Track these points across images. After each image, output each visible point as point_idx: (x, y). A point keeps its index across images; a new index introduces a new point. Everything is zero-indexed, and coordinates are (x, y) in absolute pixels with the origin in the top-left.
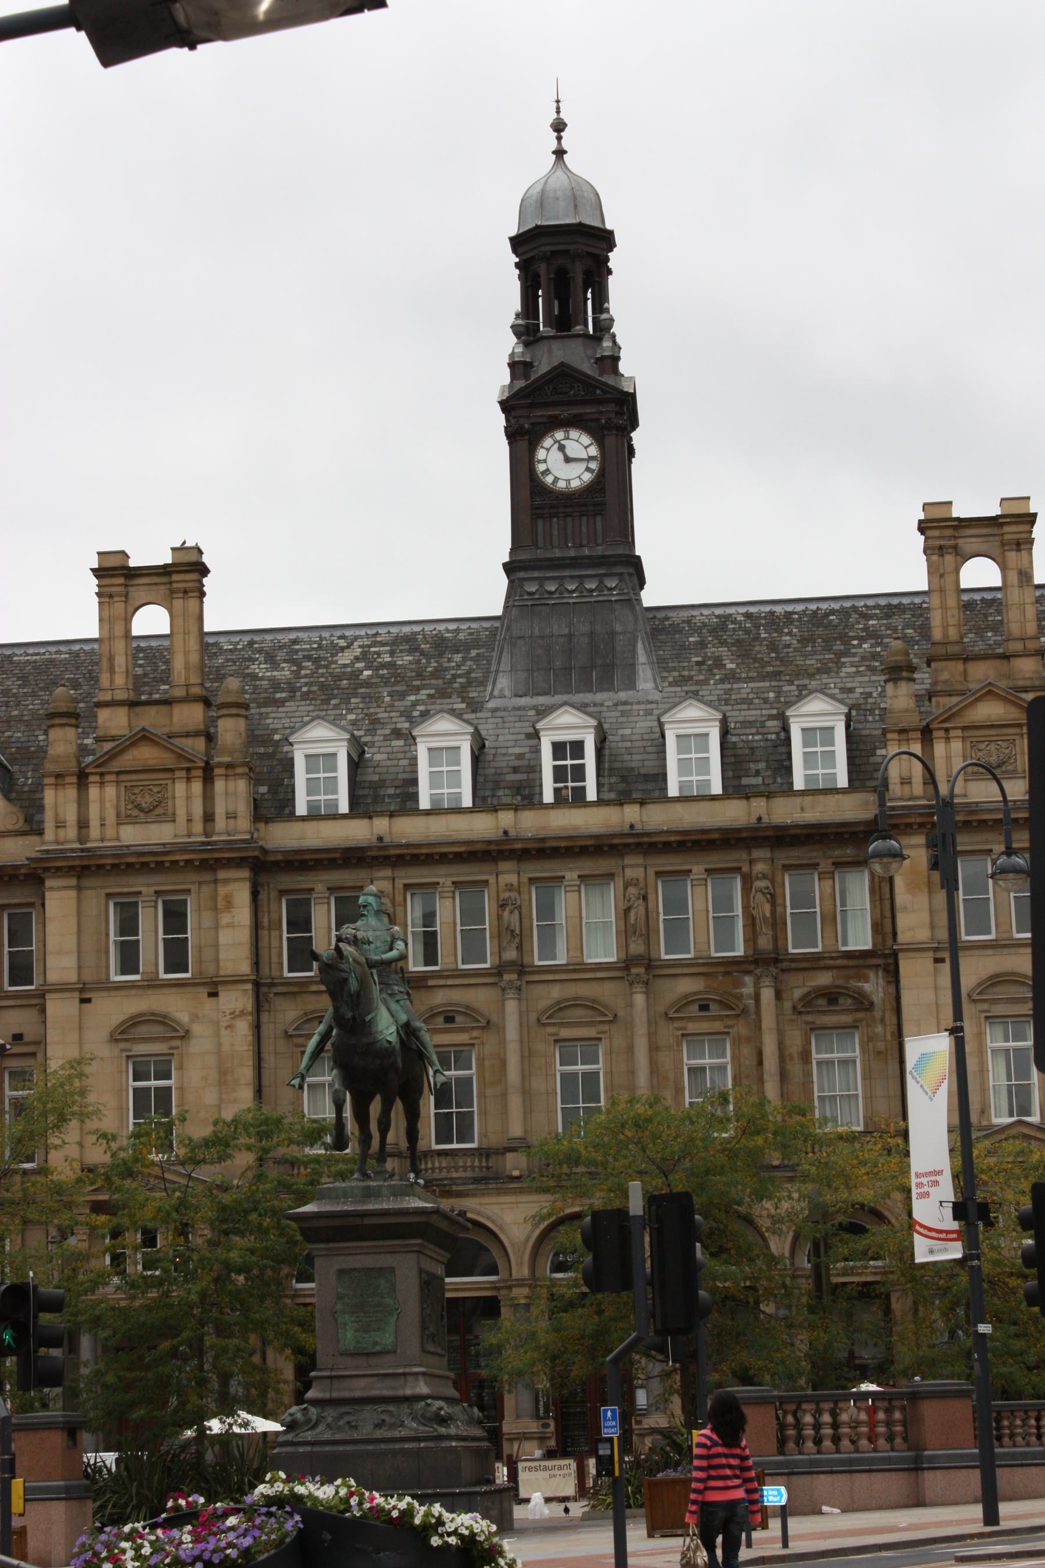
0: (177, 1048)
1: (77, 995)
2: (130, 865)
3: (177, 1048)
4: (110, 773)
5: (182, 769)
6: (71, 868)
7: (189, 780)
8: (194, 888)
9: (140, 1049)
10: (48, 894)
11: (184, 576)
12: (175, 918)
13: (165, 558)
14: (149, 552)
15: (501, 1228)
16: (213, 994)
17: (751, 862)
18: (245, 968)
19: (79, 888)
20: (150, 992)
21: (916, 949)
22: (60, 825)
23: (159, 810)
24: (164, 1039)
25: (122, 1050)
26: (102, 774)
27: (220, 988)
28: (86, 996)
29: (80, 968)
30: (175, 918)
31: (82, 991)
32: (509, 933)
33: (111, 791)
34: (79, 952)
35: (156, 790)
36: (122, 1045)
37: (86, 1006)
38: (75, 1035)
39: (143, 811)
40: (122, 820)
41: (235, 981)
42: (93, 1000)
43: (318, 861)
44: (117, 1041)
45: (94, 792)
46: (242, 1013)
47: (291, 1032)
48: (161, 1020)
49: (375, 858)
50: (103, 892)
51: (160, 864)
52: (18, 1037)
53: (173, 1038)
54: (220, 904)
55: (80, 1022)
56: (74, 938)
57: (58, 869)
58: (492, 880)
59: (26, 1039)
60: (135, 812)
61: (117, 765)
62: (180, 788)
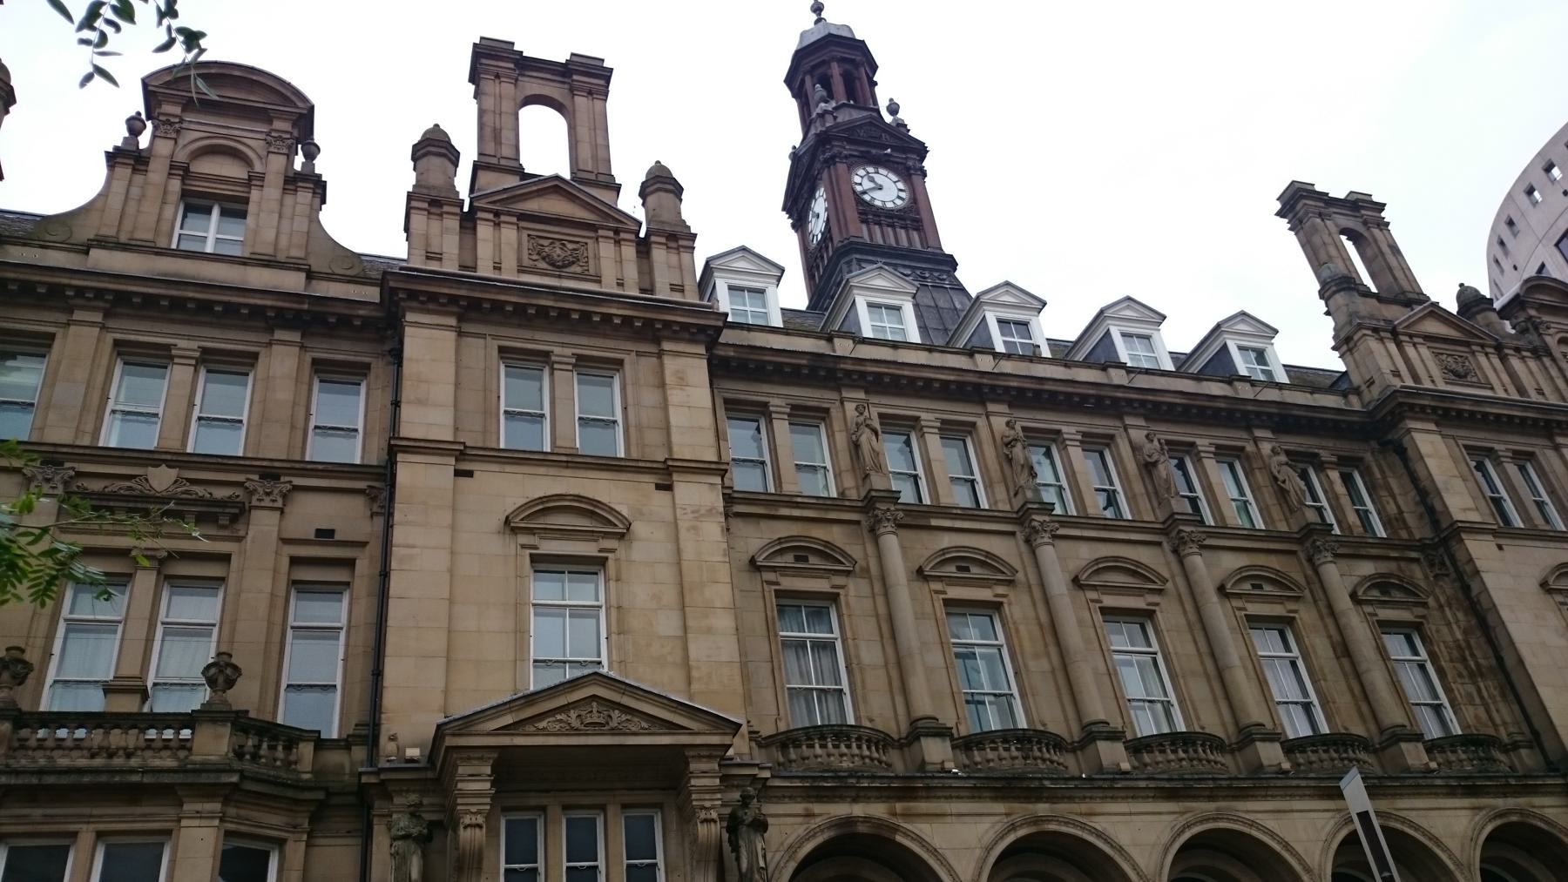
1: (452, 461)
2: (543, 311)
4: (509, 214)
5: (609, 229)
6: (454, 299)
7: (618, 243)
8: (628, 359)
10: (408, 331)
11: (580, 83)
13: (562, 57)
14: (546, 42)
15: (1120, 850)
17: (1256, 441)
19: (461, 334)
20: (568, 472)
21: (1475, 529)
26: (497, 214)
27: (675, 477)
29: (456, 429)
32: (1026, 471)
33: (509, 234)
34: (455, 406)
35: (570, 246)
36: (524, 539)
37: (463, 481)
38: (446, 517)
39: (553, 265)
40: (522, 270)
42: (476, 474)
43: (779, 367)
44: (515, 531)
46: (711, 511)
47: (760, 561)
49: (848, 373)
50: (496, 344)
51: (586, 316)
53: (606, 535)
55: (454, 500)
56: (451, 388)
57: (433, 297)
58: (981, 422)
59: (337, 537)
60: (542, 265)
62: (606, 249)
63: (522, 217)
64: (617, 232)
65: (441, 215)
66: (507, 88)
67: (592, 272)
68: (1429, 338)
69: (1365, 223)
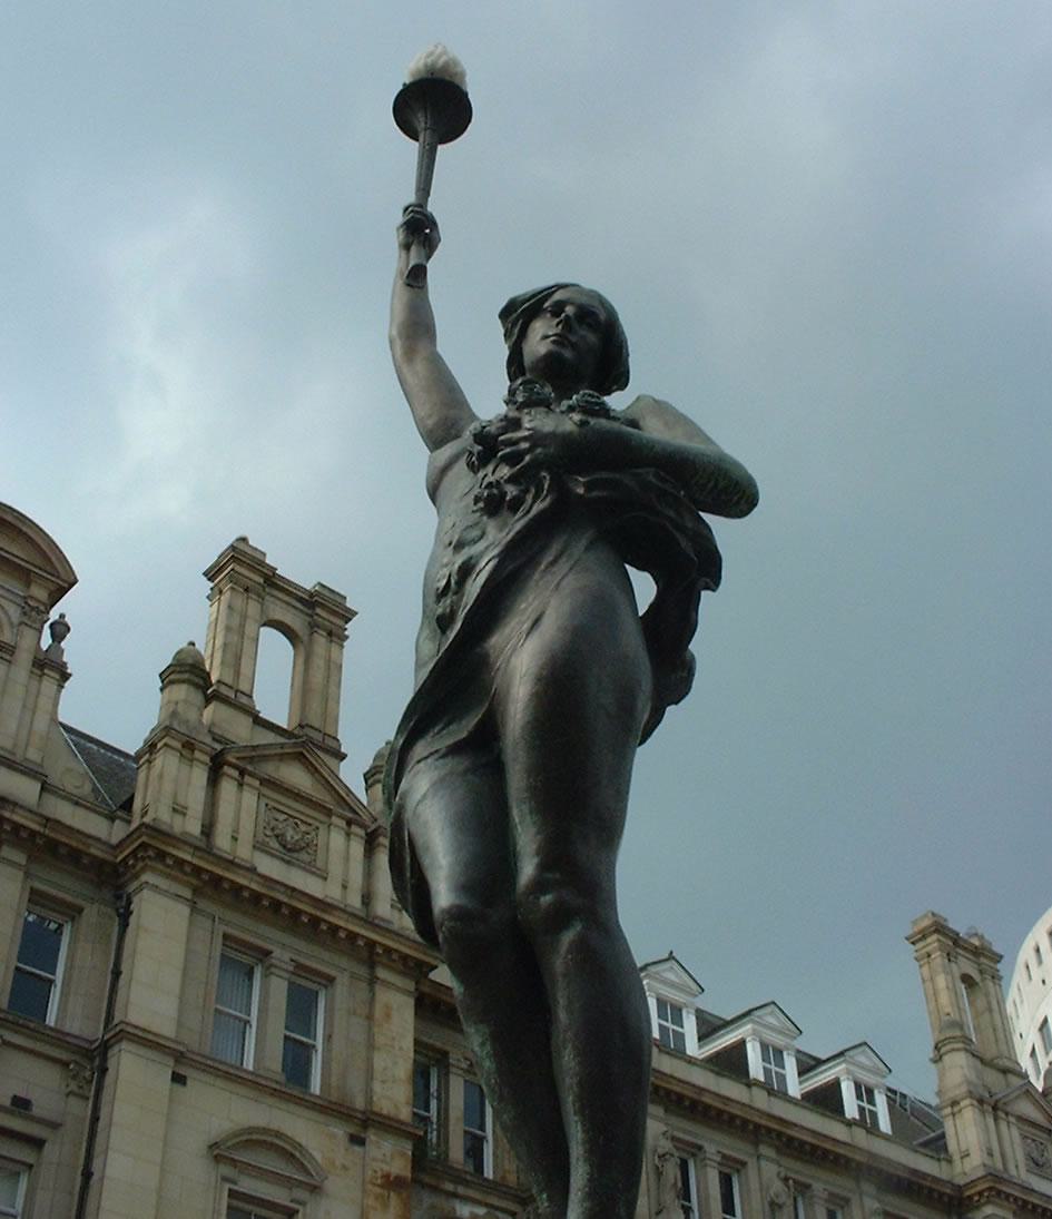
0: (303, 1203)
1: (171, 1063)
3: (303, 1203)
9: (248, 1185)
12: (301, 1009)
13: (308, 583)
14: (300, 570)
16: (357, 1140)
18: (405, 1114)
22: (179, 810)
23: (304, 856)
24: (288, 1182)
25: (225, 1179)
26: (242, 772)
28: (182, 1071)
30: (301, 1009)
31: (179, 1057)
33: (249, 798)
35: (303, 828)
36: (226, 1170)
37: (177, 1087)
39: (284, 847)
40: (259, 846)
41: (388, 1125)
45: (228, 788)
48: (290, 1152)
51: (315, 921)
52: (21, 1104)
54: (378, 1013)
56: (179, 975)
60: (274, 844)
61: (270, 769)
62: (337, 839)
63: (269, 783)
64: (349, 823)
65: (192, 760)
66: (253, 608)
67: (319, 864)
68: (1021, 1119)
69: (981, 972)
